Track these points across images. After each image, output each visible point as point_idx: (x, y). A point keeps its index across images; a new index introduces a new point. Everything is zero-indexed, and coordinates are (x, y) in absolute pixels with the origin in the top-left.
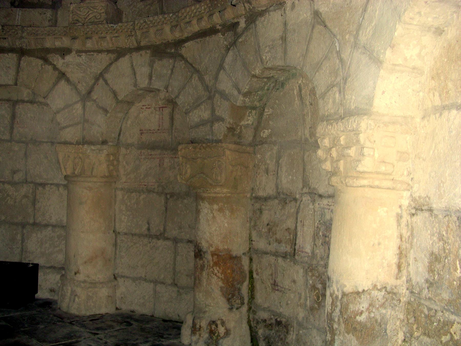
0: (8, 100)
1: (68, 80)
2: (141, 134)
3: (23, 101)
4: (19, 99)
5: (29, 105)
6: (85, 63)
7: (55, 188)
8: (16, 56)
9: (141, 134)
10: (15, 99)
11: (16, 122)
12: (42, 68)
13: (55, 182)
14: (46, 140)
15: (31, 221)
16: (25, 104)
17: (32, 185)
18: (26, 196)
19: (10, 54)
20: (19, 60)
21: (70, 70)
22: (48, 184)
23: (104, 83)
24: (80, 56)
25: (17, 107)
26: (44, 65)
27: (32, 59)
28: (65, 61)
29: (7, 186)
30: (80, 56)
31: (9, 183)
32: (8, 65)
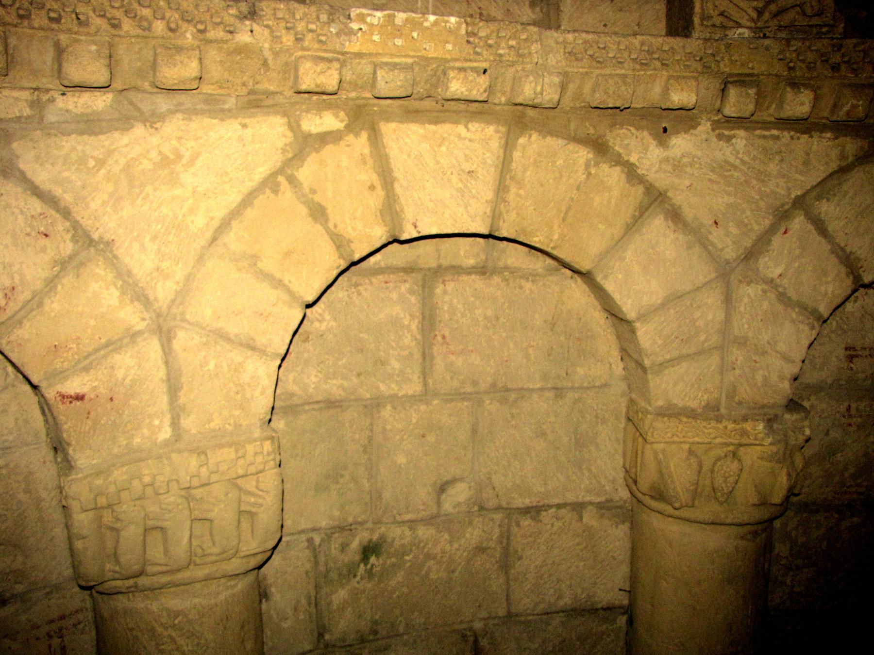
0: (409, 270)
1: (675, 216)
2: (851, 358)
3: (457, 270)
4: (445, 262)
5: (476, 282)
6: (743, 162)
7: (570, 515)
8: (497, 132)
9: (851, 358)
10: (434, 265)
11: (439, 338)
12: (589, 174)
13: (570, 498)
14: (538, 386)
15: (502, 612)
16: (464, 278)
17: (498, 516)
18: (481, 549)
19: (474, 126)
20: (508, 146)
21: (687, 183)
22: (550, 506)
23: (810, 227)
24: (729, 139)
25: (439, 291)
26: (597, 165)
27: (553, 142)
28: (670, 153)
29: (423, 532)
30: (729, 139)
31: (429, 521)
32: (467, 167)
